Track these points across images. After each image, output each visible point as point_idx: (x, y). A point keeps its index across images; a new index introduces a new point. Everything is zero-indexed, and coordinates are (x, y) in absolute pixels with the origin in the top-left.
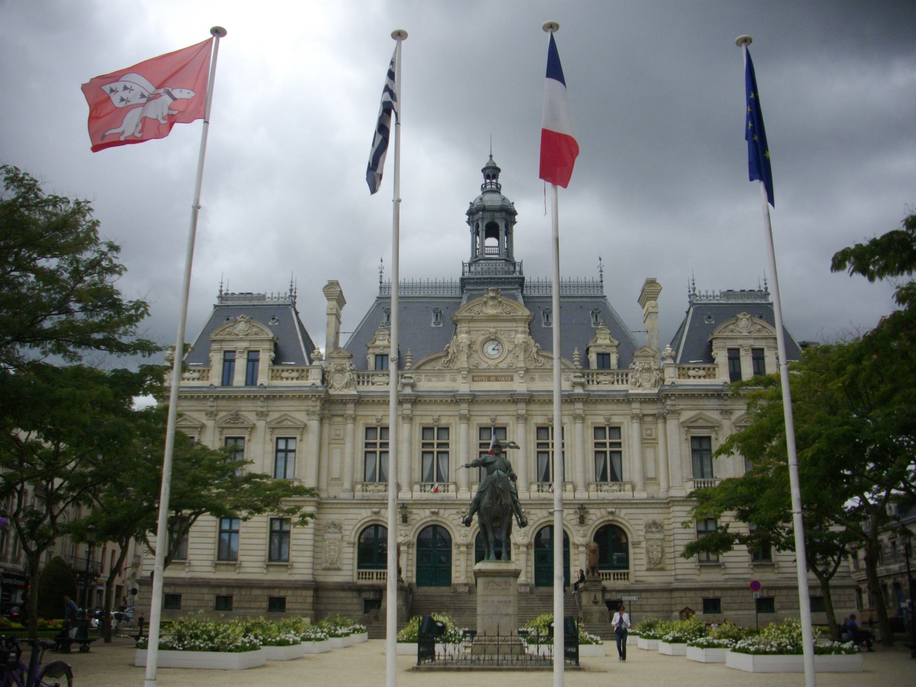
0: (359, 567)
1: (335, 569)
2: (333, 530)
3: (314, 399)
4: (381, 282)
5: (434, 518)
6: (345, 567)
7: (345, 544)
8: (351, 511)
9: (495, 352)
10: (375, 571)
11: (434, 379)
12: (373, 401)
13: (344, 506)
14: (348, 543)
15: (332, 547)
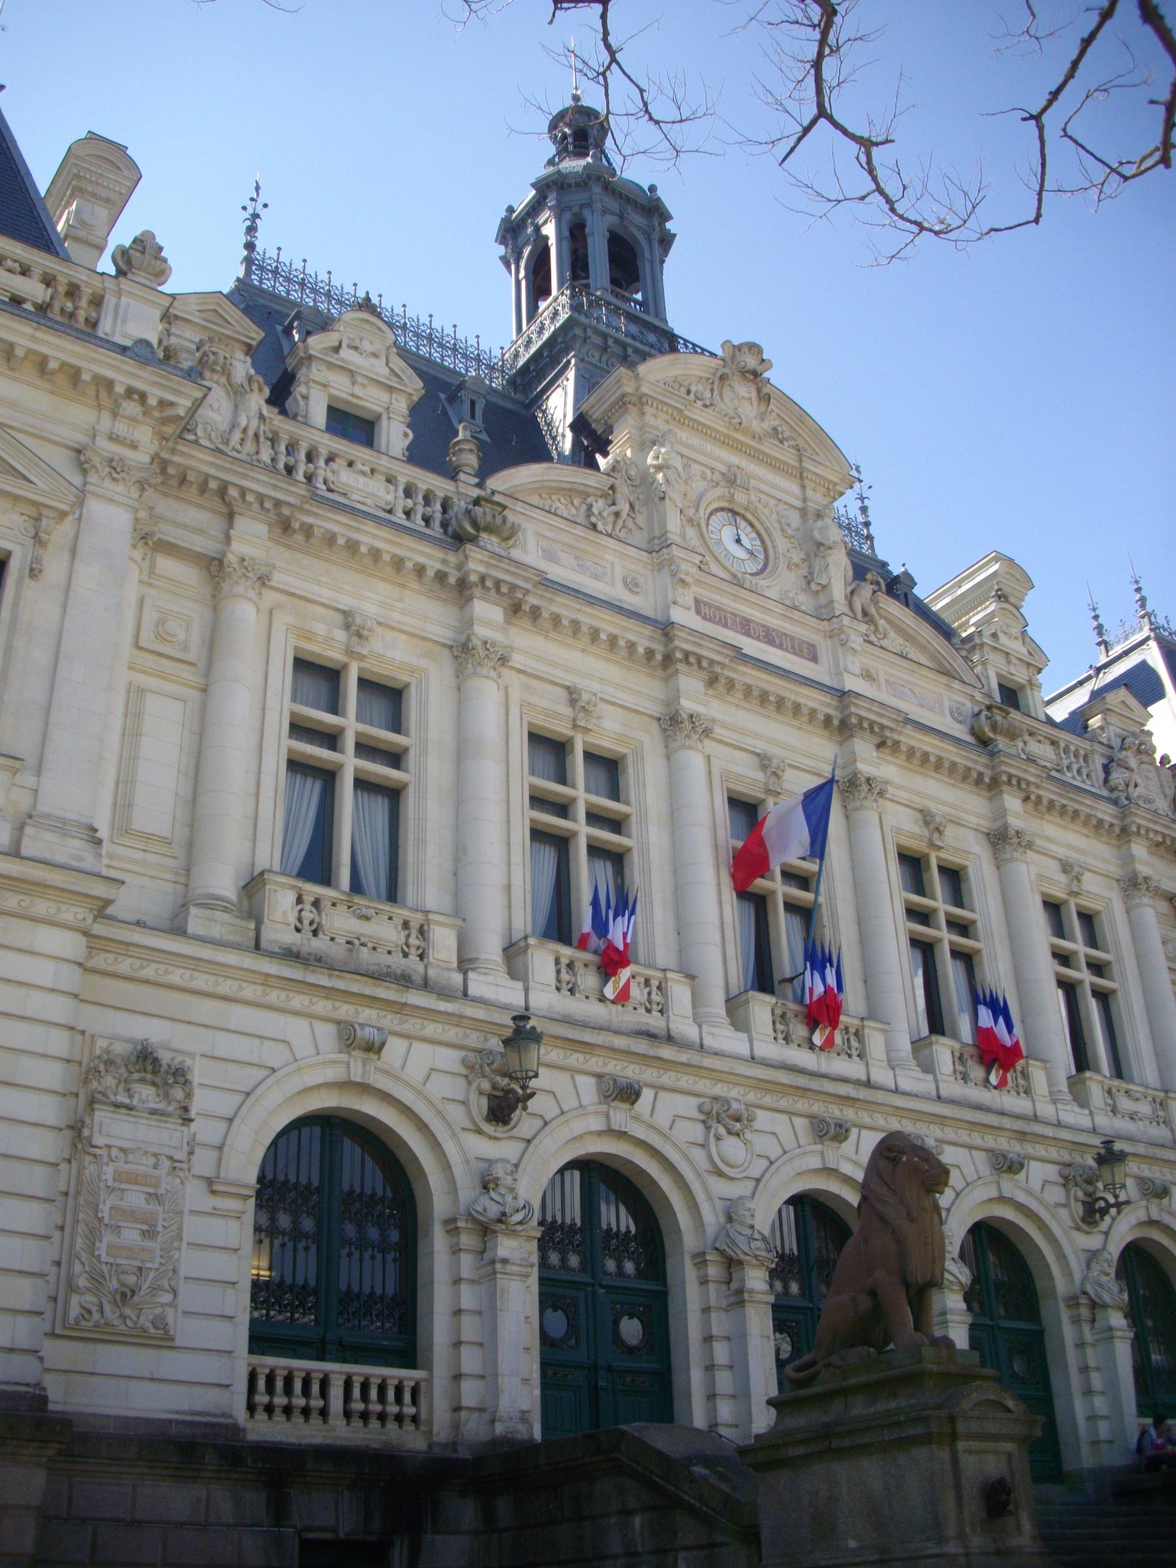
0: (262, 1340)
1: (140, 1338)
2: (146, 1094)
3: (131, 408)
4: (250, 246)
5: (620, 1116)
6: (187, 1331)
7: (194, 1195)
8: (240, 1016)
9: (739, 552)
10: (337, 1370)
11: (567, 558)
12: (352, 547)
13: (201, 982)
14: (211, 1184)
15: (135, 1199)
